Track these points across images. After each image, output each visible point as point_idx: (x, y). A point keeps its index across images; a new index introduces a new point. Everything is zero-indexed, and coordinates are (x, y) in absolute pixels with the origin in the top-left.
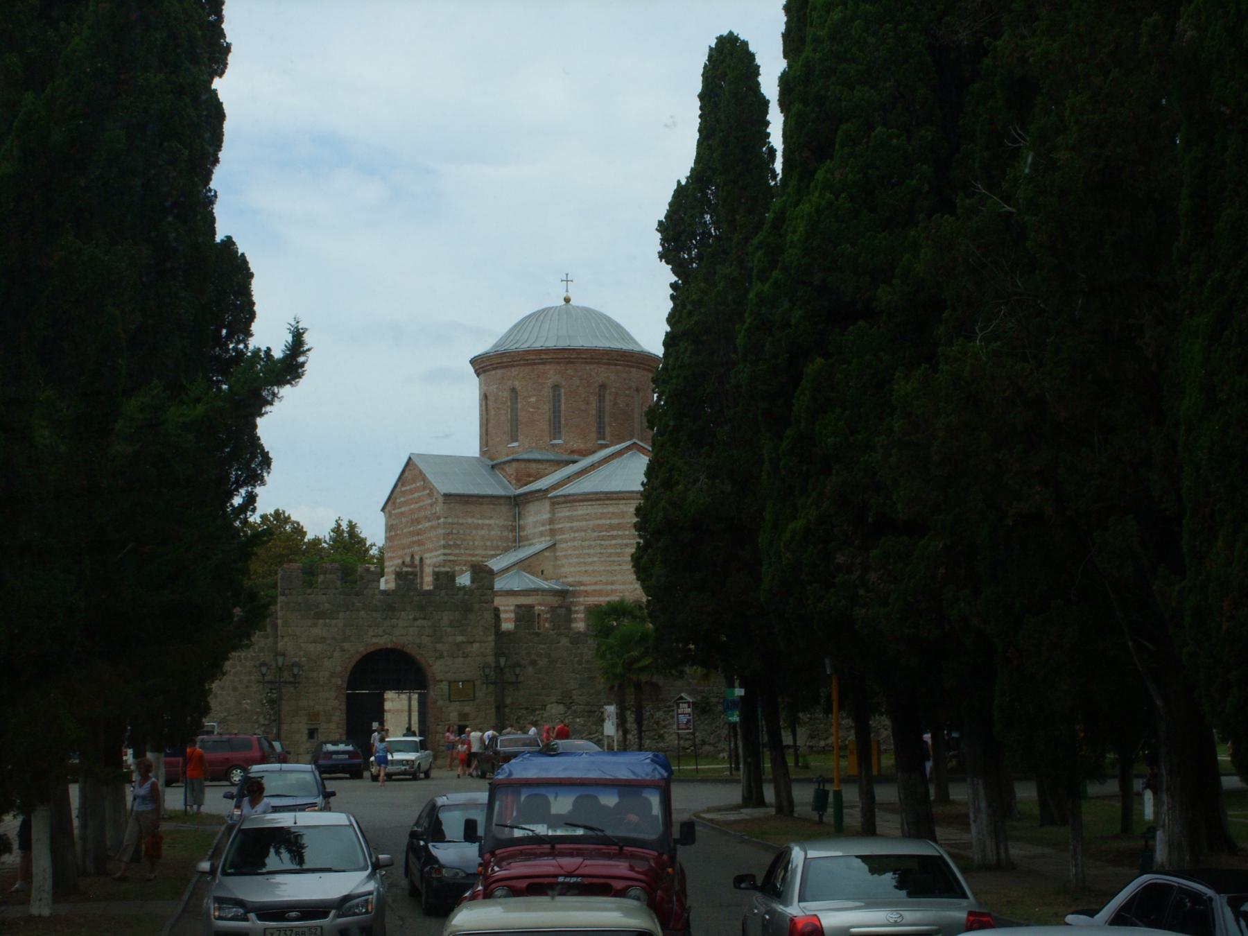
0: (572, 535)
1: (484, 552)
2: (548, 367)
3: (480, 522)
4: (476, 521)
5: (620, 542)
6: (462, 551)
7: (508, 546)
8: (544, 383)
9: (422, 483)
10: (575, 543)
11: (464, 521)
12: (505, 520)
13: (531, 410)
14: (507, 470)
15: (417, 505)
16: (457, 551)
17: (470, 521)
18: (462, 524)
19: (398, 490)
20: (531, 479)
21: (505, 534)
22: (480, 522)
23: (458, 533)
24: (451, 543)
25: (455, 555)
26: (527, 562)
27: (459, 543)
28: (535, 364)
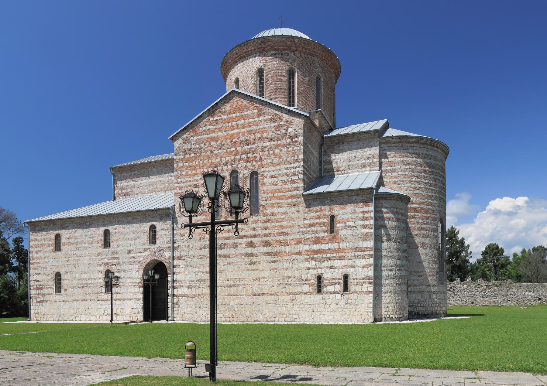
0: (403, 167)
13: (306, 86)
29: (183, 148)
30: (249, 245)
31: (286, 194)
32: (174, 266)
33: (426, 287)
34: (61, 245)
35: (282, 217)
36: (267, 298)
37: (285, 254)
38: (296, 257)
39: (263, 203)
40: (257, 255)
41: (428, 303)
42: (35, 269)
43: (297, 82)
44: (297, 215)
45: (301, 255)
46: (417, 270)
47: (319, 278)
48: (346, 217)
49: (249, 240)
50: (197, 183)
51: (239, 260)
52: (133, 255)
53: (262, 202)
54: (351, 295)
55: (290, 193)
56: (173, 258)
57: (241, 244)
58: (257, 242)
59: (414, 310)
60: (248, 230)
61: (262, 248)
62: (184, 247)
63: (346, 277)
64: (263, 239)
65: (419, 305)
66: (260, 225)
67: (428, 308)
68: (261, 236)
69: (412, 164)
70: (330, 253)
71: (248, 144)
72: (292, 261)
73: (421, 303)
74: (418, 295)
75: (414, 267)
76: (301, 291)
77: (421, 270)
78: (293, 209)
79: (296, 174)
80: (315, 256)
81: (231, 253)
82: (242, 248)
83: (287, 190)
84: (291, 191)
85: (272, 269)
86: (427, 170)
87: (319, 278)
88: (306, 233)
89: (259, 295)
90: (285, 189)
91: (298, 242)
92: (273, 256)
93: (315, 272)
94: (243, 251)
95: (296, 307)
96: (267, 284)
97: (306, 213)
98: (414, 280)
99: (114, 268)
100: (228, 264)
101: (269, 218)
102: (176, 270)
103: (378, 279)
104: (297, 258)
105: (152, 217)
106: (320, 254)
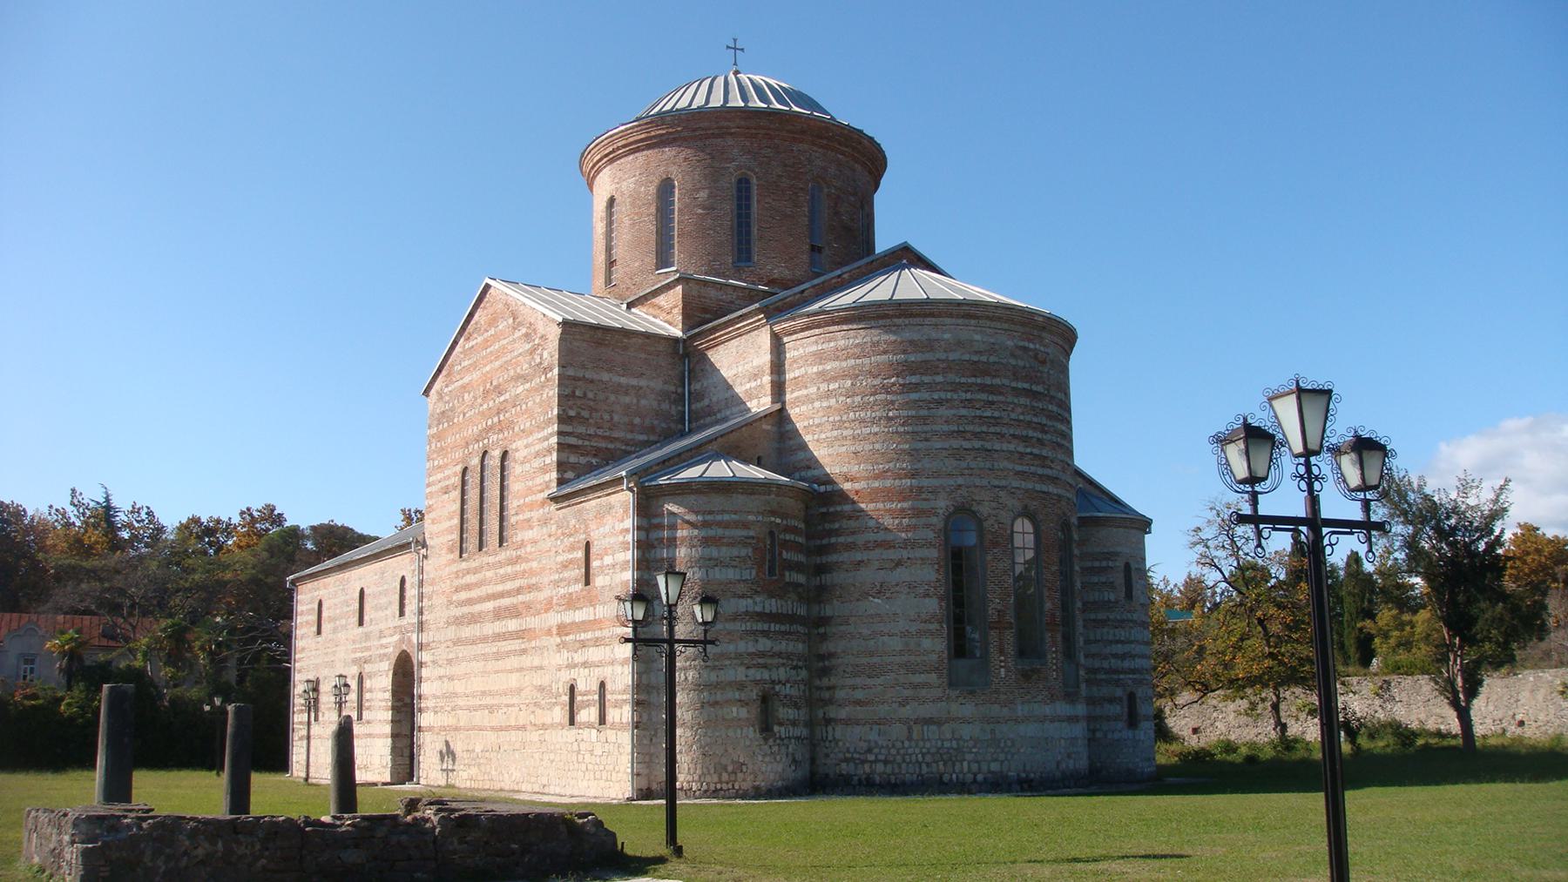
0: (824, 387)
1: (629, 436)
2: (730, 141)
3: (623, 380)
4: (616, 379)
5: (926, 396)
6: (591, 431)
7: (669, 428)
8: (724, 168)
9: (511, 321)
10: (833, 401)
11: (595, 377)
12: (665, 383)
14: (663, 303)
15: (497, 364)
16: (581, 429)
17: (605, 376)
18: (592, 381)
19: (458, 349)
20: (708, 316)
21: (665, 406)
22: (623, 380)
23: (585, 394)
24: (572, 413)
25: (579, 436)
26: (735, 435)
27: (585, 414)
28: (708, 137)
29: (438, 411)
30: (498, 615)
32: (421, 664)
33: (895, 706)
35: (533, 550)
36: (514, 736)
39: (513, 520)
41: (902, 752)
42: (300, 671)
43: (679, 208)
44: (549, 543)
46: (864, 661)
48: (607, 542)
50: (447, 483)
52: (384, 641)
54: (608, 731)
56: (421, 647)
58: (507, 608)
59: (858, 772)
63: (602, 685)
65: (871, 757)
66: (509, 569)
67: (904, 765)
68: (508, 594)
69: (844, 377)
70: (584, 632)
71: (501, 394)
73: (876, 751)
74: (867, 727)
75: (855, 653)
77: (875, 660)
78: (545, 529)
79: (549, 451)
80: (567, 638)
85: (521, 669)
86: (894, 384)
87: (572, 688)
88: (556, 583)
89: (507, 728)
91: (549, 606)
92: (520, 641)
93: (566, 677)
94: (490, 628)
96: (513, 705)
98: (854, 688)
99: (368, 668)
102: (425, 672)
103: (656, 694)
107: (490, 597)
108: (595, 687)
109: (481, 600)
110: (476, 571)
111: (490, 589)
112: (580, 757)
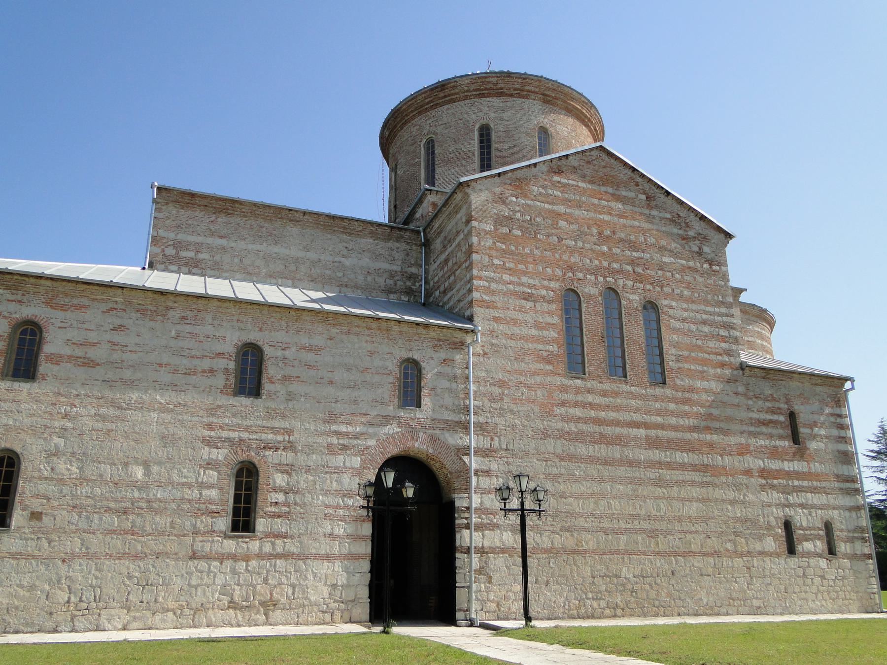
30: (654, 443)
31: (713, 357)
34: (42, 358)
37: (723, 471)
38: (744, 479)
40: (669, 466)
44: (736, 400)
45: (752, 476)
47: (788, 526)
49: (653, 433)
51: (638, 473)
53: (671, 363)
55: (720, 358)
57: (636, 438)
58: (670, 441)
60: (648, 412)
61: (678, 455)
62: (500, 426)
64: (679, 435)
66: (672, 406)
68: (675, 428)
72: (738, 487)
76: (761, 549)
80: (775, 482)
81: (617, 455)
82: (640, 447)
83: (713, 350)
84: (721, 355)
87: (788, 526)
88: (755, 435)
90: (709, 347)
92: (702, 474)
93: (779, 513)
94: (643, 455)
95: (757, 584)
97: (750, 399)
100: (612, 479)
101: (687, 395)
104: (745, 481)
105: (410, 340)
106: (783, 479)
107: (637, 425)
108: (820, 524)
109: (616, 423)
110: (604, 394)
111: (637, 417)
112: (809, 582)
